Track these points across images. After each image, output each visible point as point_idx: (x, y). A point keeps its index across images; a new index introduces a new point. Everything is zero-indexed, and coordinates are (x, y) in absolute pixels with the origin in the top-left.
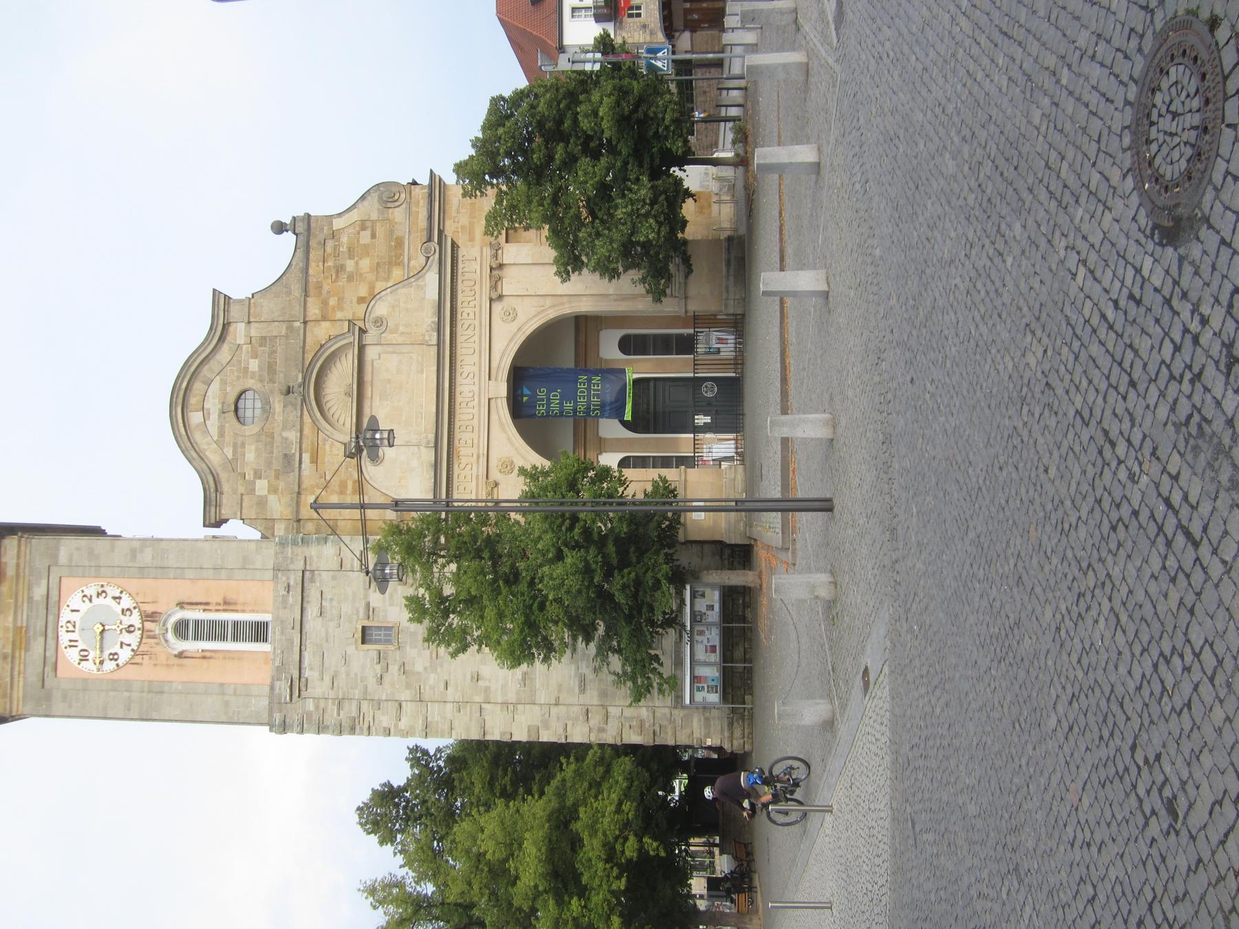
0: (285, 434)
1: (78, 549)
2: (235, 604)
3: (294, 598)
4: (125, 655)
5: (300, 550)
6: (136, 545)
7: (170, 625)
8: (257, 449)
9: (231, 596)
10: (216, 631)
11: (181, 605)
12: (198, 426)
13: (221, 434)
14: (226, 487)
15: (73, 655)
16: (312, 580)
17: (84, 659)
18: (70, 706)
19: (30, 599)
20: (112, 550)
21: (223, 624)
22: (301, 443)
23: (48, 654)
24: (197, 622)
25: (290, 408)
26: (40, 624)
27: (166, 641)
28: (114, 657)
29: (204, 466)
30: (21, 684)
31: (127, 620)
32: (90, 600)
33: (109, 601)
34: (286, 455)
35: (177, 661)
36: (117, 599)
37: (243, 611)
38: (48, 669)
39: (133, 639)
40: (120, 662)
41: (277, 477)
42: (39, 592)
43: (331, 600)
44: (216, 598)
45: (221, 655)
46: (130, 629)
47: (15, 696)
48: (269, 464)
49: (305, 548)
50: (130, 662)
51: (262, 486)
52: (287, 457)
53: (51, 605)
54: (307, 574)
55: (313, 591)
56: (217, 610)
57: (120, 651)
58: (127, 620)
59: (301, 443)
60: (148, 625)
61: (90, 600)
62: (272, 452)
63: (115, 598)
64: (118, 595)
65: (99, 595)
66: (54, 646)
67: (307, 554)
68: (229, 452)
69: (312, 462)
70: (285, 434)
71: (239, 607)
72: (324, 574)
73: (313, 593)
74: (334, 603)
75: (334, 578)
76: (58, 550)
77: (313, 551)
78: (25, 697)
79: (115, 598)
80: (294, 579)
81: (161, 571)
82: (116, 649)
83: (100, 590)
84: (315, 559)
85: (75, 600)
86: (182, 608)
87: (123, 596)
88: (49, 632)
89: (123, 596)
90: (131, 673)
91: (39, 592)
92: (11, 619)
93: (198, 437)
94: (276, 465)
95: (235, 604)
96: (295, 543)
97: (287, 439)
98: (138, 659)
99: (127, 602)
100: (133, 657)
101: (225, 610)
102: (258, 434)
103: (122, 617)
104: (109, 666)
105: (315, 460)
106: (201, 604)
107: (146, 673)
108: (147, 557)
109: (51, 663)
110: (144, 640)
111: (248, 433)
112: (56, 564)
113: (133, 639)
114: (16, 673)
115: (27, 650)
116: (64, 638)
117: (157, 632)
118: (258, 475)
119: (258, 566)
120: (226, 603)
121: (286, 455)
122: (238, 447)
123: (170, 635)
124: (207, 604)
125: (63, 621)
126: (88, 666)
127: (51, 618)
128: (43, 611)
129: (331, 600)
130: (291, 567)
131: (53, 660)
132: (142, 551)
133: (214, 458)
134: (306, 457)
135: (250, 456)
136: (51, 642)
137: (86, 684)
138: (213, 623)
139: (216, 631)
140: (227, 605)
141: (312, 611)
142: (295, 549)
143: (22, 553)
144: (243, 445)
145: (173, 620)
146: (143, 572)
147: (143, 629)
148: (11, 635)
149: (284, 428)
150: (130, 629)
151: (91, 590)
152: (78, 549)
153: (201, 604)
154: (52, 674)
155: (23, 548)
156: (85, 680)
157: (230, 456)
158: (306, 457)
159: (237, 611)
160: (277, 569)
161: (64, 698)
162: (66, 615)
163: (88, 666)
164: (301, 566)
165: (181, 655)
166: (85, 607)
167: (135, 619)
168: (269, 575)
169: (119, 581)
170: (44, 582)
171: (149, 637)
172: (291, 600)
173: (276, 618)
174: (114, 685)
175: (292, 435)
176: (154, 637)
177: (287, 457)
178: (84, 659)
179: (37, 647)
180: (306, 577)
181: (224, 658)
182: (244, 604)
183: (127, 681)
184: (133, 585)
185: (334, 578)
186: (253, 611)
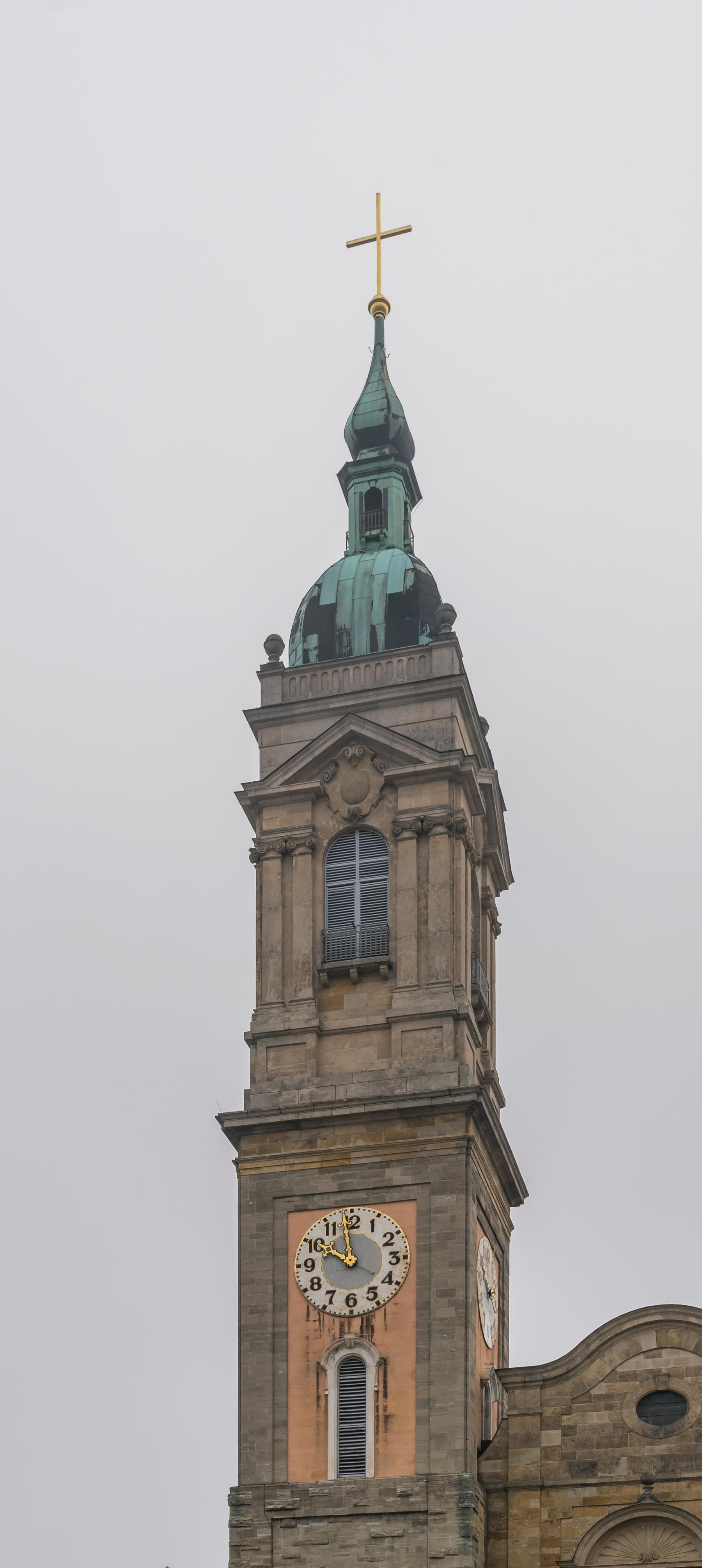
0: (624, 1461)
1: (453, 1218)
2: (386, 1430)
3: (393, 1503)
4: (319, 1298)
5: (452, 1504)
6: (460, 1295)
7: (356, 1351)
8: (603, 1426)
9: (394, 1425)
10: (352, 1410)
11: (383, 1363)
12: (638, 1345)
13: (625, 1377)
14: (550, 1392)
15: (317, 1231)
16: (416, 1523)
17: (313, 1245)
18: (251, 1237)
19: (387, 1164)
20: (452, 1264)
21: (362, 1418)
22: (611, 1484)
23: (316, 1198)
24: (363, 1383)
25: (659, 1464)
26: (353, 1182)
27: (337, 1350)
28: (316, 1284)
29: (579, 1360)
30: (278, 1169)
31: (361, 1293)
32: (387, 1244)
33: (386, 1268)
34: (594, 1465)
35: (313, 1365)
36: (389, 1279)
37: (376, 1441)
38: (298, 1201)
39: (339, 1306)
40: (310, 1294)
41: (564, 1457)
42: (396, 1175)
43: (392, 1549)
44: (393, 1405)
45: (322, 1419)
46: (350, 1300)
47: (261, 1164)
48: (583, 1445)
49: (455, 1512)
50: (309, 1305)
51: (553, 1438)
52: (591, 1467)
53: (380, 1194)
54: (422, 1517)
55: (403, 1525)
56: (377, 1408)
57: (323, 1291)
58: (361, 1293)
59: (611, 1484)
60: (357, 1323)
61: (387, 1244)
62: (599, 1446)
63: (390, 1275)
64: (394, 1279)
65: (394, 1254)
66: (326, 1204)
67: (448, 1516)
68: (601, 1390)
69: (585, 1500)
70: (624, 1461)
71: (381, 1435)
72: (422, 1537)
73: (398, 1527)
74: (388, 1553)
75: (419, 1549)
76: (452, 1192)
77: (453, 1521)
78: (262, 1176)
79: (390, 1275)
80: (417, 1502)
81: (426, 1331)
82: (326, 1286)
83: (400, 1255)
84: (442, 1525)
85: (385, 1225)
86: (379, 1365)
87: (394, 1286)
88: (346, 1197)
89: (394, 1286)
90: (296, 1308)
91: (396, 1175)
92: (360, 1143)
93: (621, 1346)
94: (582, 1455)
95: (386, 1430)
96: (462, 1498)
97: (617, 1464)
98: (314, 1315)
99: (385, 1292)
100: (316, 1308)
101: (377, 1418)
102: (624, 1426)
103: (366, 1288)
104: (304, 1278)
105: (587, 1503)
106: (385, 1387)
107: (297, 1325)
108: (444, 1311)
109: (308, 1202)
110: (337, 1321)
111: (625, 1412)
112: (433, 1193)
113: (339, 1306)
114: (291, 1161)
115: (321, 1170)
116: (336, 1217)
117: (347, 1337)
118: (568, 1431)
119: (434, 1454)
120: (387, 1417)
121: (594, 1465)
122: (607, 1402)
123: (344, 1353)
124: (385, 1395)
125: (359, 1211)
126: (303, 1253)
127: (363, 1195)
128: (370, 1183)
129: (392, 1549)
130: (432, 1497)
131: (310, 1207)
132: (451, 1303)
133: (592, 1372)
134: (592, 1492)
135: (597, 1418)
136: (333, 1199)
137: (280, 1252)
138: (361, 1404)
139: (352, 1410)
140: (385, 1420)
141: (377, 1527)
142: (455, 1500)
143: (446, 1145)
144: (609, 1407)
145: (364, 1354)
146: (423, 1307)
147: (352, 1316)
148: (339, 1146)
149: (632, 1460)
150: (350, 1300)
151: (400, 1244)
152: (453, 1218)
153: (385, 1387)
154: (291, 1206)
155: (453, 1144)
156: (286, 1251)
157: (594, 1392)
158: (592, 1492)
159: (377, 1432)
160: (428, 1479)
161: (261, 1228)
162: (366, 1214)
163: (303, 1253)
164: (434, 1507)
165: (320, 1371)
166: (378, 1238)
167: (364, 1305)
168: (423, 1469)
169: (413, 1278)
170: (408, 1180)
171: (342, 1326)
172: (390, 1499)
173: (367, 1483)
174: (280, 1291)
175: (622, 1471)
176: (342, 1332)
177: (591, 1467)
178: (313, 1245)
179: (326, 1183)
180: (419, 1517)
181: (318, 1424)
182: (386, 1441)
183: (287, 1305)
184: (409, 1297)
185: (419, 1549)
186: (377, 1452)
